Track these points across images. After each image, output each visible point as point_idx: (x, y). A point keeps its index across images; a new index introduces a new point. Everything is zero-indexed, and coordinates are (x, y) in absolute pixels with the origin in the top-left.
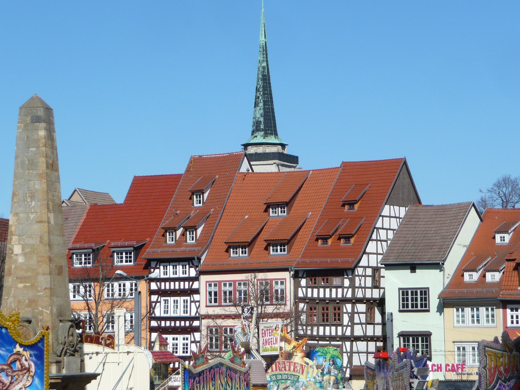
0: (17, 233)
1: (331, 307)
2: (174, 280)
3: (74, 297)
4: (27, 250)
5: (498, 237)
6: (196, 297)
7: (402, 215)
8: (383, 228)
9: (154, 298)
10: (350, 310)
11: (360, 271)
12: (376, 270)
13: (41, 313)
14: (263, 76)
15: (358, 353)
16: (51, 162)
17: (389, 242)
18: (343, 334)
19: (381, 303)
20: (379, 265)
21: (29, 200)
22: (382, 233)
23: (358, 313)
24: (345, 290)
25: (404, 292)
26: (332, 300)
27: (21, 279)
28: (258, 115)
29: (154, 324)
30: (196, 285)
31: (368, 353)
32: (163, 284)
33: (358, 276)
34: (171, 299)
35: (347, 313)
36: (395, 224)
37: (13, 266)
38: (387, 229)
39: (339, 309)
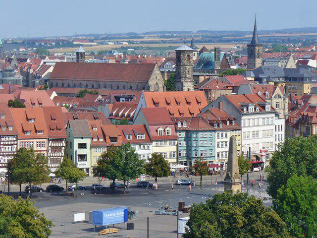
2: (9, 141)
6: (15, 146)
30: (16, 143)
34: (7, 147)
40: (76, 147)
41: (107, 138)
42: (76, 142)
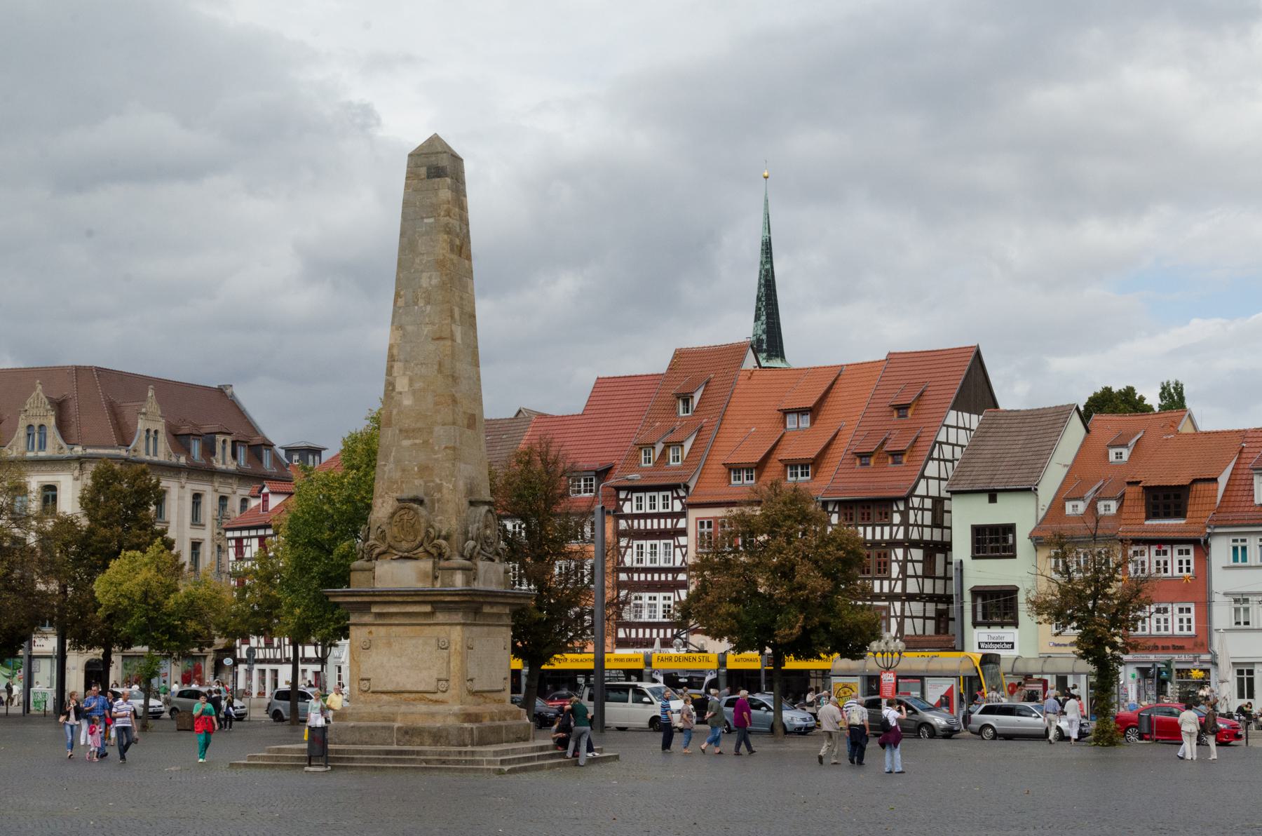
0: (402, 357)
1: (874, 553)
2: (652, 516)
4: (418, 385)
5: (1112, 454)
6: (683, 540)
7: (975, 426)
8: (947, 443)
9: (623, 543)
10: (900, 557)
11: (916, 502)
12: (938, 501)
13: (439, 488)
14: (767, 281)
15: (912, 617)
16: (458, 242)
17: (956, 463)
18: (891, 591)
19: (946, 547)
20: (944, 494)
21: (421, 303)
22: (947, 450)
23: (913, 561)
24: (895, 529)
25: (978, 531)
26: (875, 544)
27: (406, 432)
28: (760, 332)
29: (623, 577)
30: (682, 524)
31: (925, 618)
33: (913, 508)
34: (647, 544)
35: (897, 561)
36: (963, 438)
37: (395, 412)
38: (953, 445)
39: (885, 555)
40: (962, 547)
42: (966, 516)
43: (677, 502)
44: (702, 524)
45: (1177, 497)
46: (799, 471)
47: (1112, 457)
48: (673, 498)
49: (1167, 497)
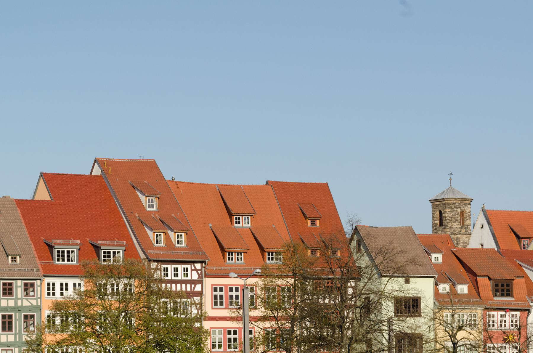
2: (176, 282)
3: (62, 294)
6: (197, 299)
30: (198, 288)
32: (174, 285)
41: (483, 282)
43: (194, 273)
44: (215, 290)
45: (508, 285)
46: (274, 257)
47: (433, 260)
48: (192, 270)
49: (502, 285)
